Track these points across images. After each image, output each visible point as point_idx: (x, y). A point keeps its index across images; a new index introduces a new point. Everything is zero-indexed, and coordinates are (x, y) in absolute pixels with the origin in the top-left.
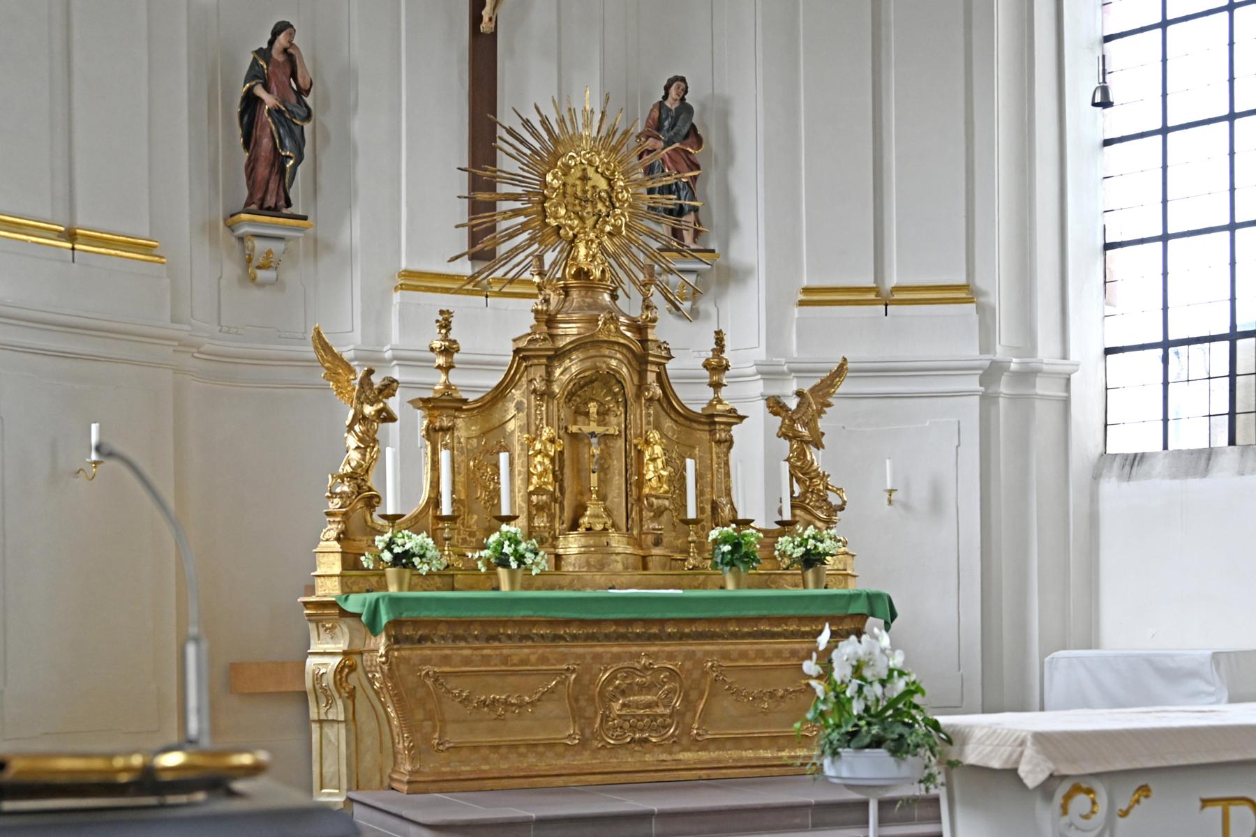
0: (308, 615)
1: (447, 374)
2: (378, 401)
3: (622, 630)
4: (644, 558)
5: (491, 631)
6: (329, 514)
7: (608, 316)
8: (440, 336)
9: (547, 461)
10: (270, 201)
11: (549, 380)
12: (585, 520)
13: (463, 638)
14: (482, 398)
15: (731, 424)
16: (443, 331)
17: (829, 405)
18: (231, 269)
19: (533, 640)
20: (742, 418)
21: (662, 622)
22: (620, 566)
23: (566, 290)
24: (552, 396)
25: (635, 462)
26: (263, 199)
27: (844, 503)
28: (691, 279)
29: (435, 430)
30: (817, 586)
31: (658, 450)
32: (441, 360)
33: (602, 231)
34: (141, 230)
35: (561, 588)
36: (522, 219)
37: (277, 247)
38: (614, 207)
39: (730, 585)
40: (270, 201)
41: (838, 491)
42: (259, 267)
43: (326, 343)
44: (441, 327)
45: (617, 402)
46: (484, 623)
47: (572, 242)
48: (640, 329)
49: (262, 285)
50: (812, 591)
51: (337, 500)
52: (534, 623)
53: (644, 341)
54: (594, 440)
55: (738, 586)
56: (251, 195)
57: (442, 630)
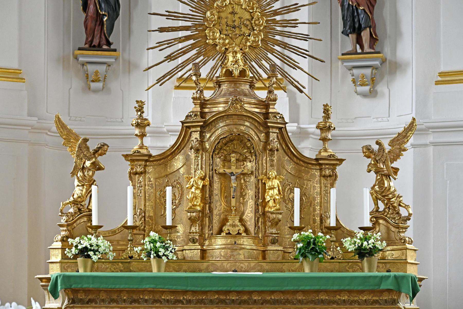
0: (42, 286)
1: (142, 139)
2: (92, 158)
3: (222, 297)
4: (264, 251)
5: (135, 297)
6: (61, 226)
7: (234, 99)
8: (137, 117)
9: (198, 192)
10: (96, 42)
11: (202, 141)
12: (225, 228)
13: (116, 301)
14: (164, 153)
15: (336, 165)
16: (139, 113)
17: (405, 150)
18: (77, 83)
19: (161, 303)
20: (341, 161)
21: (250, 293)
22: (242, 257)
24: (204, 150)
25: (261, 190)
26: (92, 41)
27: (410, 215)
28: (368, 72)
29: (136, 173)
30: (370, 271)
31: (276, 182)
32: (137, 131)
33: (245, 45)
34: (14, 65)
35: (200, 271)
36: (192, 41)
38: (254, 30)
39: (307, 270)
40: (96, 42)
41: (406, 207)
42: (93, 81)
43: (63, 124)
44: (137, 111)
45: (251, 152)
46: (129, 292)
47: (224, 54)
48: (266, 105)
49: (96, 91)
50: (366, 273)
51: (64, 218)
52: (163, 292)
53: (266, 115)
54: (233, 178)
55: (312, 271)
56: (87, 39)
57: (103, 296)
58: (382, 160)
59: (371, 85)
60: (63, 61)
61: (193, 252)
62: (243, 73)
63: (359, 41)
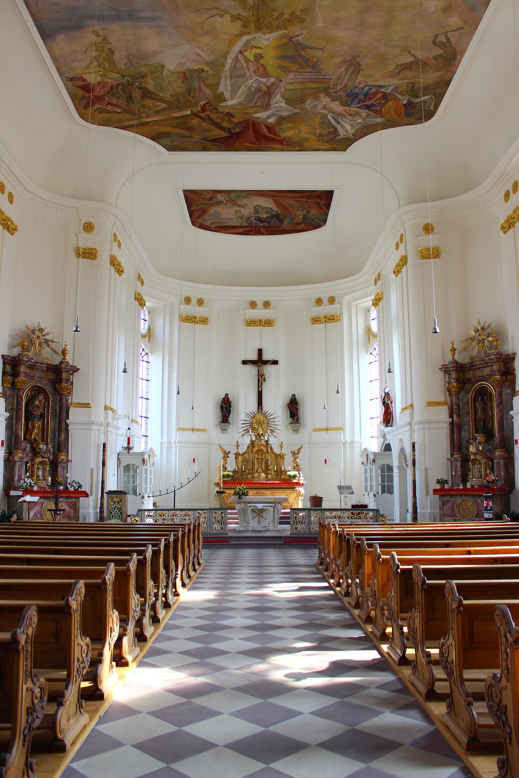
18: (220, 431)
23: (256, 437)
28: (296, 428)
37: (226, 427)
48: (267, 442)
58: (295, 454)
59: (296, 431)
60: (216, 425)
61: (250, 476)
62: (262, 434)
63: (294, 419)
